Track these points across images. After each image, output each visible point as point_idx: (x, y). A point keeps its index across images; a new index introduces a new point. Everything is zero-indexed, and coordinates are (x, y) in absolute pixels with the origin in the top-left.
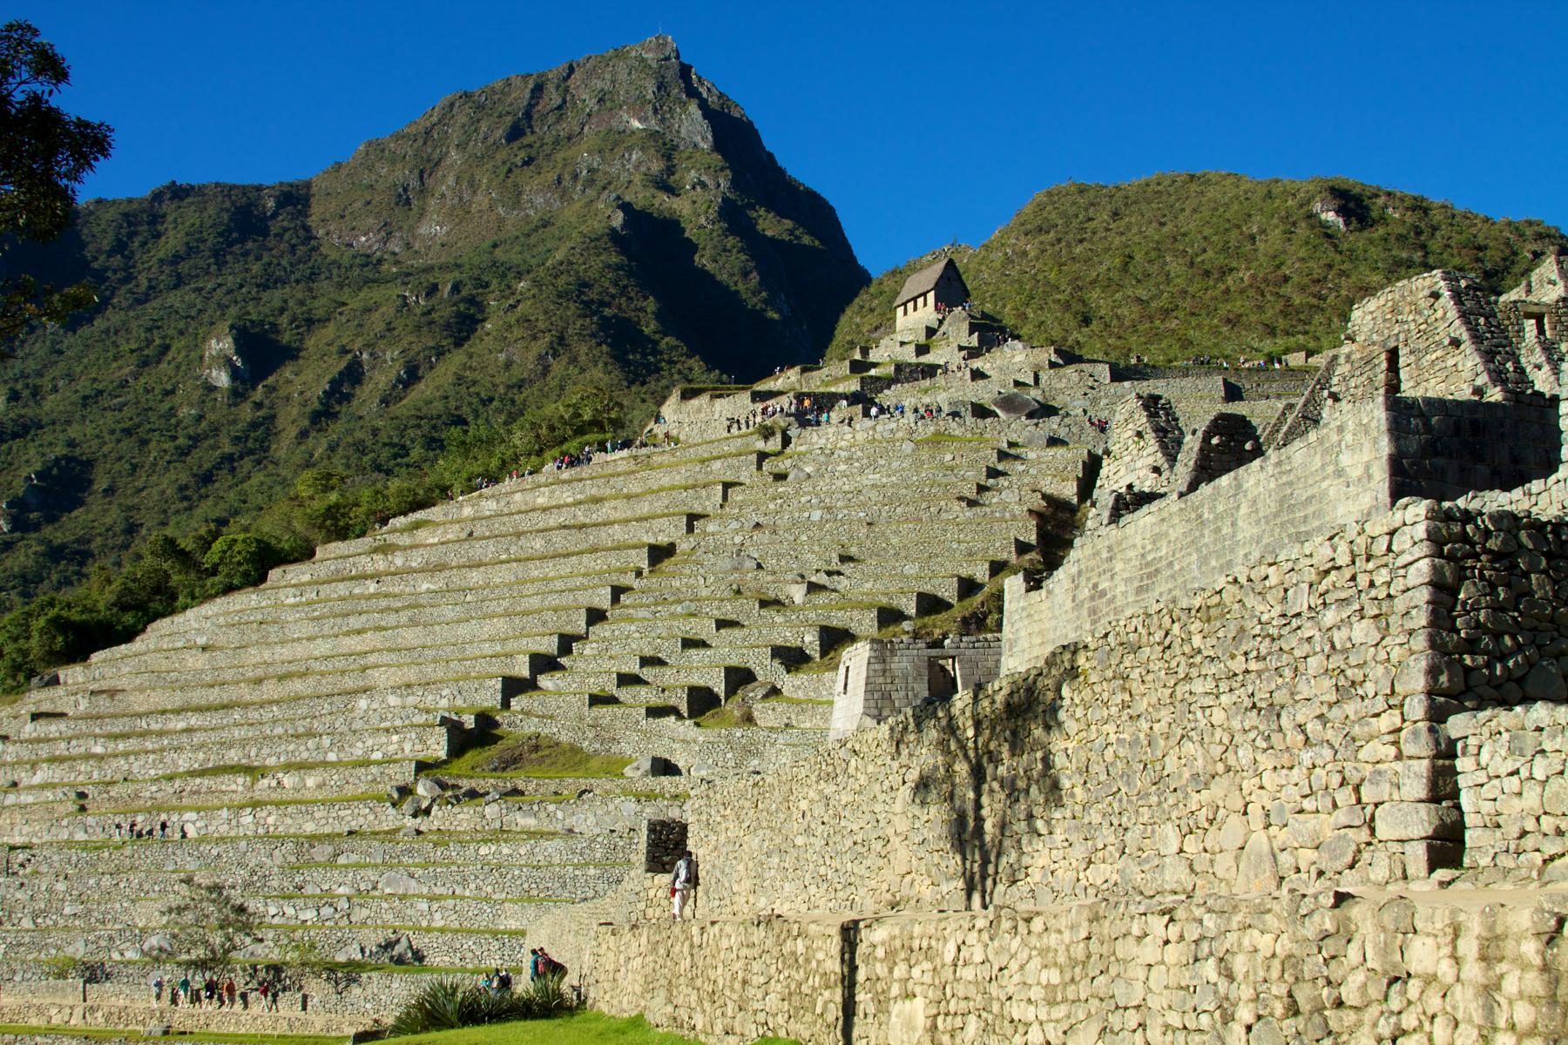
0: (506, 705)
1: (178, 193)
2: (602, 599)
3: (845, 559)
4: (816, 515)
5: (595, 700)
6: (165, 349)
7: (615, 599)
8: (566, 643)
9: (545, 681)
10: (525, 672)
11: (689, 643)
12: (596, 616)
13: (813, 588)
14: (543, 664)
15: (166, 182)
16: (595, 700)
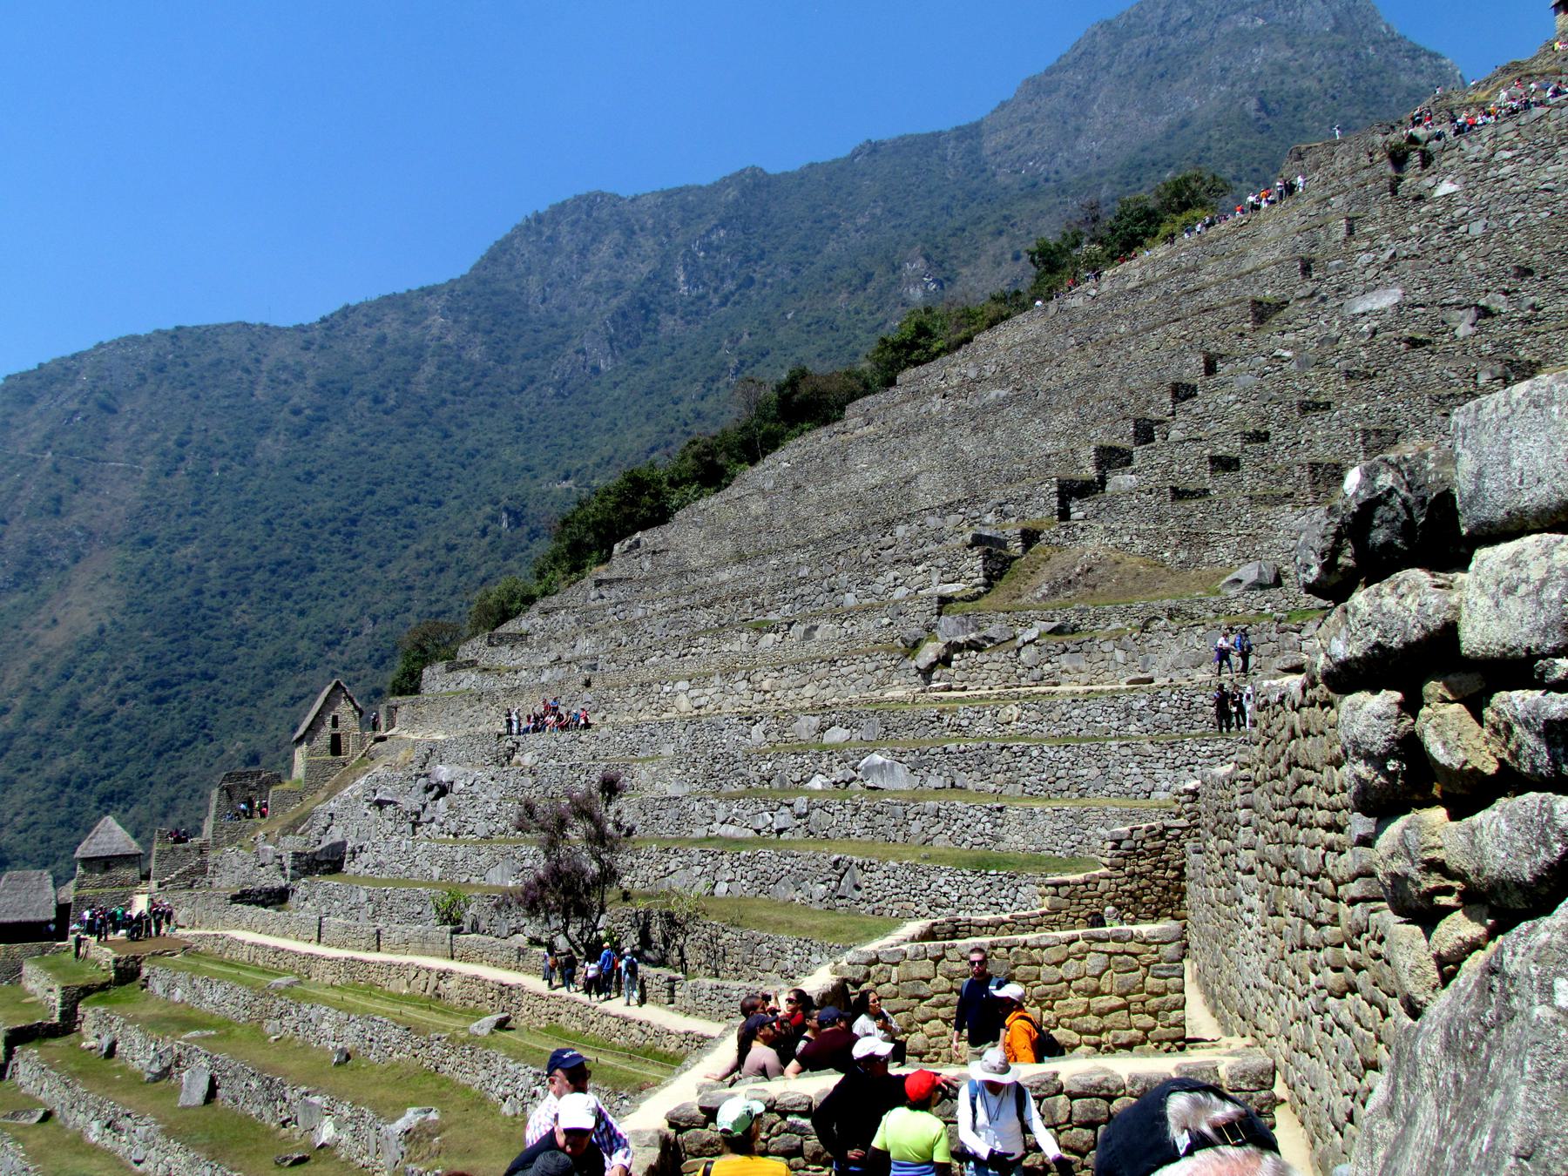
0: (1064, 515)
1: (873, 149)
2: (1192, 367)
3: (1525, 272)
4: (1477, 229)
5: (1179, 494)
6: (868, 277)
7: (1210, 369)
8: (1145, 433)
9: (1121, 481)
10: (1090, 472)
11: (1307, 408)
12: (1183, 392)
13: (1485, 312)
14: (1111, 458)
15: (859, 140)
16: (1179, 494)
